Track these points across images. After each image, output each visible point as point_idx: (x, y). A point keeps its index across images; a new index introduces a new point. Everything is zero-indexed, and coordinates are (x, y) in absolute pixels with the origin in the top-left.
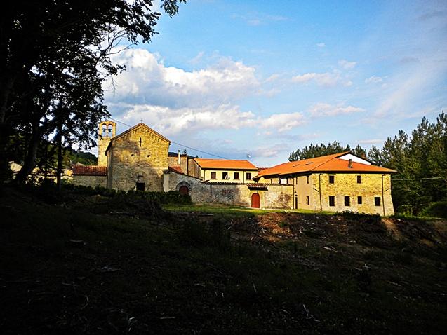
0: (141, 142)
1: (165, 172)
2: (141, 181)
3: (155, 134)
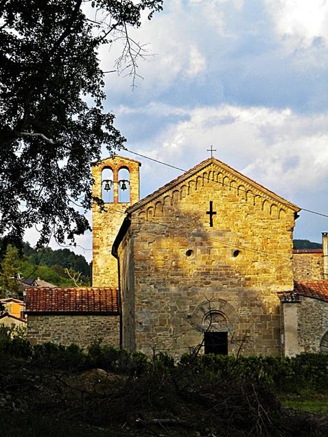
0: (211, 213)
1: (286, 299)
2: (217, 327)
3: (252, 187)
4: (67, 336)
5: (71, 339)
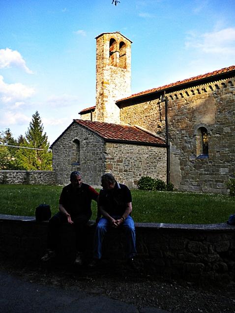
4: (134, 162)
5: (137, 166)
